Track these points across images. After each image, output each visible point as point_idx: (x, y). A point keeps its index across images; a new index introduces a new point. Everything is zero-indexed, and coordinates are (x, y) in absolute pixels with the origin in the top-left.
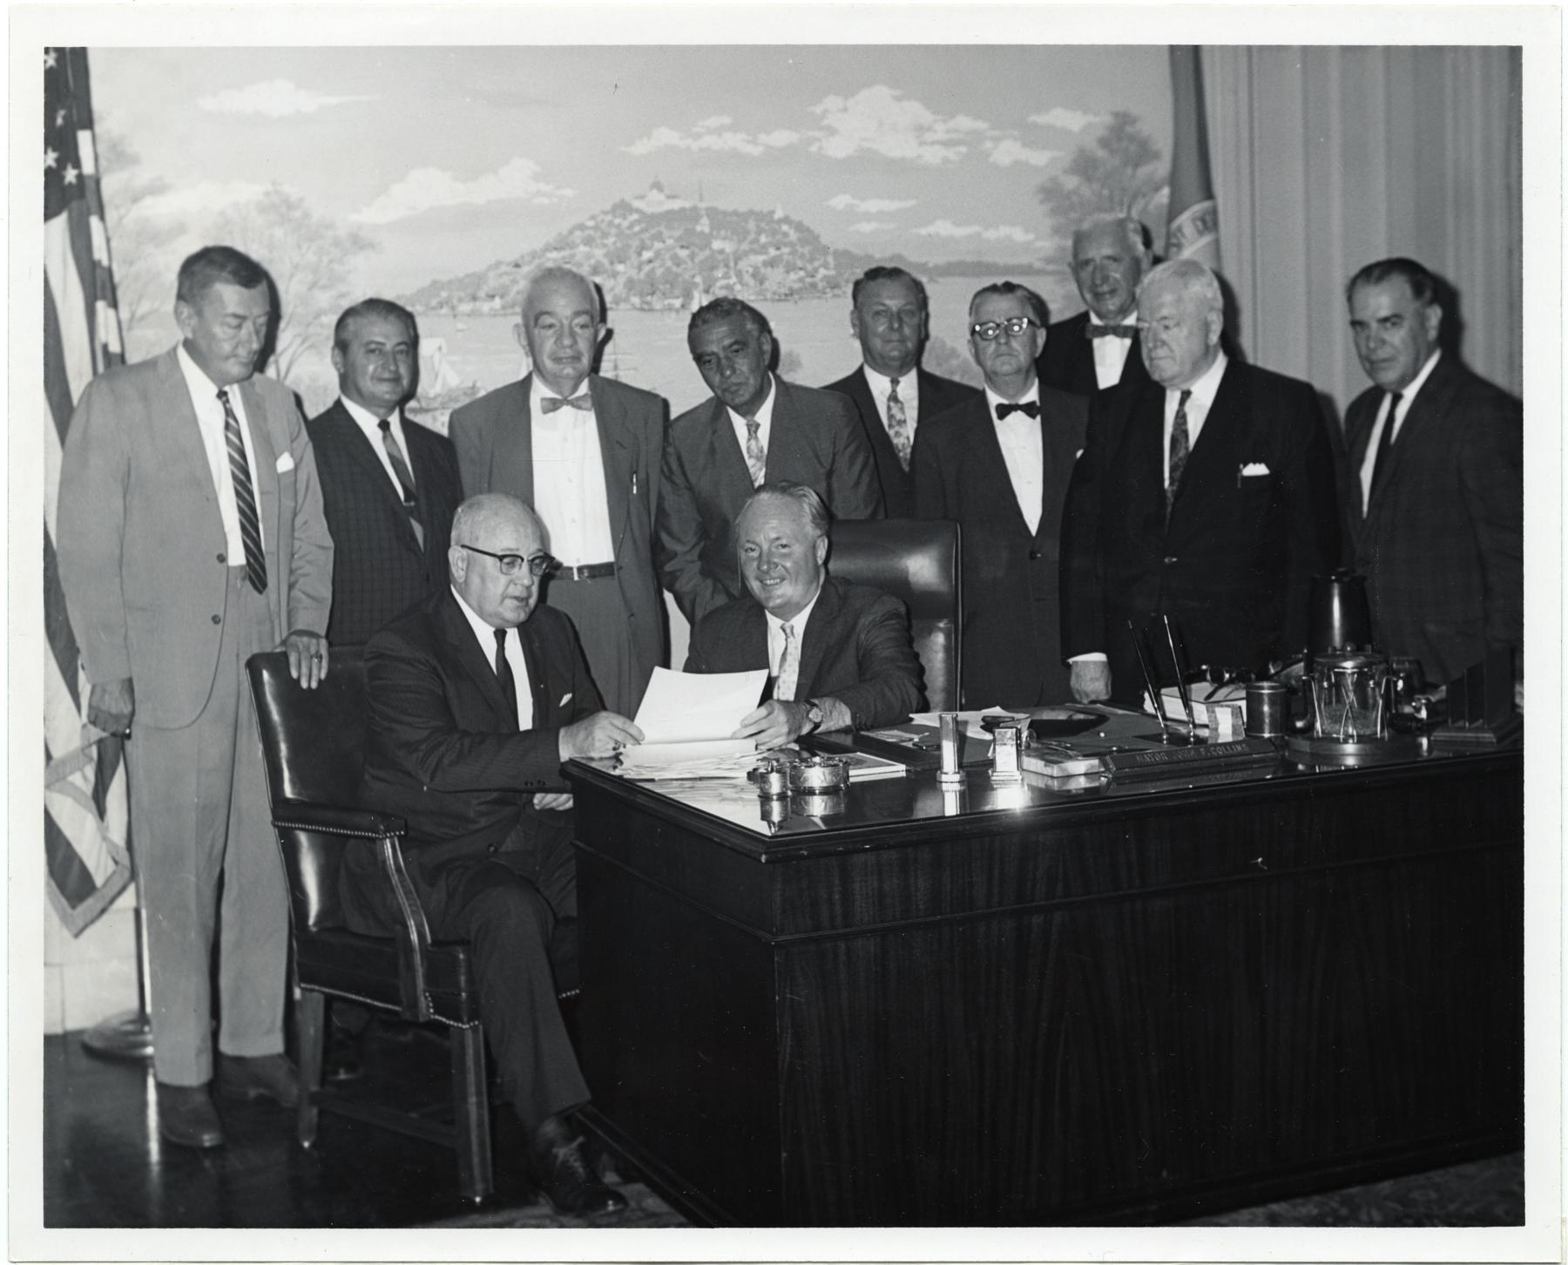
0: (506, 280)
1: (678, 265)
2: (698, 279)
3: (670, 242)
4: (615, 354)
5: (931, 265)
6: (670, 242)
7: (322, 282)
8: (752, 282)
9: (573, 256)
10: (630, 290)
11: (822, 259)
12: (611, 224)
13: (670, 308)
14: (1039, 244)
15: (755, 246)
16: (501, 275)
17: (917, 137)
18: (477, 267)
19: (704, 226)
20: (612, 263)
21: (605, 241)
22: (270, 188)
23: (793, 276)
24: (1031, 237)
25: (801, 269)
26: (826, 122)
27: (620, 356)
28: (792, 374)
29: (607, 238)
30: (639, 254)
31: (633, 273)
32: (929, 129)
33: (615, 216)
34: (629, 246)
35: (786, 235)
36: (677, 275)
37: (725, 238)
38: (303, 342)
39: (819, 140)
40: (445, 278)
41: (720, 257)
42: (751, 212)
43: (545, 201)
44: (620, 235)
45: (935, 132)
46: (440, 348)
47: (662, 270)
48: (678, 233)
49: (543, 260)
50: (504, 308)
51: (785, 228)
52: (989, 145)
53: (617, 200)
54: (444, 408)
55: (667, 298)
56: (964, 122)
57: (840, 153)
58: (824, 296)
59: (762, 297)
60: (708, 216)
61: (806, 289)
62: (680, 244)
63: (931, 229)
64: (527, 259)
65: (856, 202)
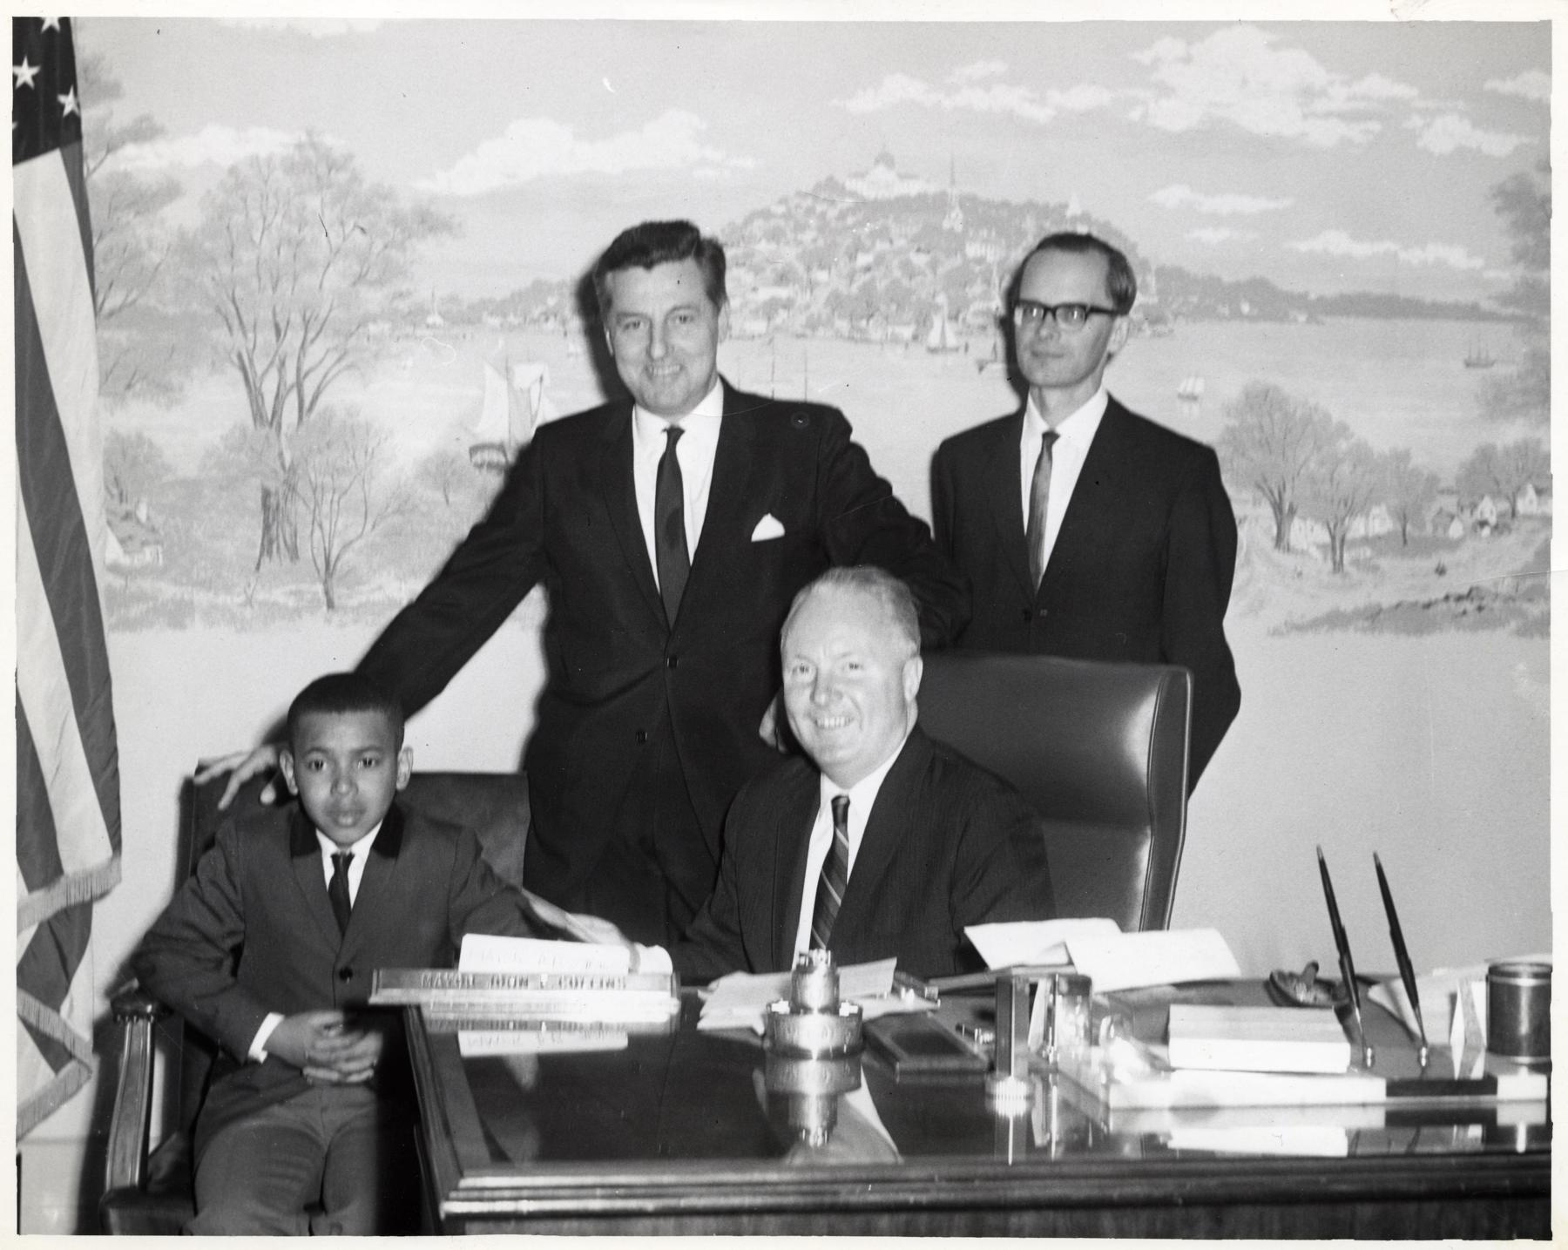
1: (911, 279)
2: (941, 299)
3: (901, 243)
5: (1313, 296)
10: (833, 310)
12: (810, 211)
13: (895, 340)
14: (1491, 274)
19: (954, 220)
20: (809, 269)
22: (304, 138)
24: (1478, 263)
30: (852, 257)
31: (842, 287)
32: (1323, 93)
37: (986, 241)
38: (339, 360)
41: (977, 269)
42: (1030, 206)
44: (823, 228)
46: (541, 379)
48: (913, 230)
52: (1417, 121)
56: (1378, 86)
62: (916, 247)
63: (1317, 244)
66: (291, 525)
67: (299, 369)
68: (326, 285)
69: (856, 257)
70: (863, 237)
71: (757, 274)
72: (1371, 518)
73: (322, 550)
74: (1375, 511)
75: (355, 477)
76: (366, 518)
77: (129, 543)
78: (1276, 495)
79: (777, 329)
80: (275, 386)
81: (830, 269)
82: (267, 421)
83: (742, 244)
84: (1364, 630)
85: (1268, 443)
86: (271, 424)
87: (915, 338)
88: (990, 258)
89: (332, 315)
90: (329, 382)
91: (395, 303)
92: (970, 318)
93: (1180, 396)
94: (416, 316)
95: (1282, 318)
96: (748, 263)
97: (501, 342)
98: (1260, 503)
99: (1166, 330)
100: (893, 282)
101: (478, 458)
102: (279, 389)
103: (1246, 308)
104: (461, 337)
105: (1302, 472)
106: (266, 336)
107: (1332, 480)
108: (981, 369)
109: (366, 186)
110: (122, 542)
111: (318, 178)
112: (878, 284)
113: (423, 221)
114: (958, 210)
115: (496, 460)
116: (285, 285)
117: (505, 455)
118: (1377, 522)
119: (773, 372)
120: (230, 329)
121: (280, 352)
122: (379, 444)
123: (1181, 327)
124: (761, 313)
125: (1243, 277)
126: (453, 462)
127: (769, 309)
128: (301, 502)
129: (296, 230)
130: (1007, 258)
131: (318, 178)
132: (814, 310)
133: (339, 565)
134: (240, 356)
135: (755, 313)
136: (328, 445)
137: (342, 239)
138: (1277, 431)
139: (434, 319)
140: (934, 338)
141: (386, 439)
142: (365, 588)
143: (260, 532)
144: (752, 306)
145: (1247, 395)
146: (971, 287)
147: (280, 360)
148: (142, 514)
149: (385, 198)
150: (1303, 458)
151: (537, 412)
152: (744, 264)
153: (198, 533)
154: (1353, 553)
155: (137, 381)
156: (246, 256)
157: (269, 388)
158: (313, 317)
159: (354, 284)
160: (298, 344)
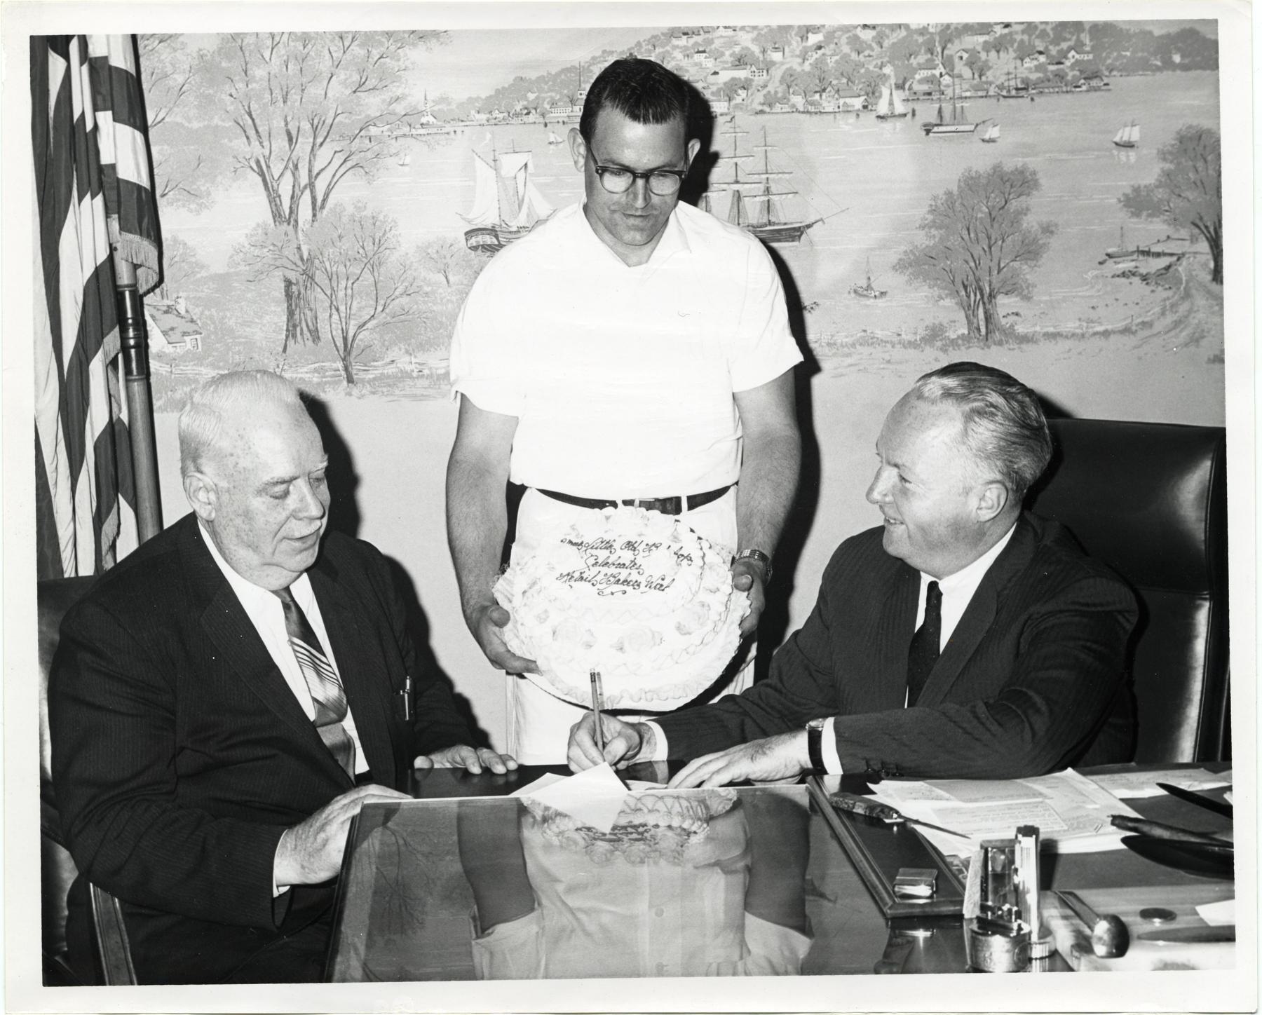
1: (859, 53)
4: (767, 173)
7: (369, 85)
8: (967, 73)
9: (711, 42)
10: (789, 87)
11: (1074, 38)
20: (764, 52)
23: (1029, 63)
25: (1041, 53)
27: (771, 176)
28: (1023, 198)
30: (804, 38)
31: (795, 64)
38: (345, 161)
40: (533, 75)
41: (921, 40)
46: (526, 165)
58: (1078, 89)
59: (980, 93)
61: (1049, 81)
66: (311, 310)
67: (310, 171)
68: (328, 95)
69: (807, 38)
71: (716, 59)
73: (340, 332)
76: (377, 302)
77: (170, 333)
78: (1212, 230)
79: (737, 106)
80: (291, 188)
82: (285, 218)
85: (1202, 182)
86: (289, 224)
87: (865, 107)
89: (336, 121)
91: (391, 108)
92: (916, 87)
93: (1117, 144)
94: (411, 117)
96: (707, 50)
98: (1197, 239)
99: (1102, 84)
100: (841, 58)
101: (473, 242)
102: (294, 192)
103: (1177, 58)
104: (452, 133)
106: (280, 143)
108: (928, 132)
110: (165, 333)
112: (829, 61)
115: (489, 243)
116: (294, 96)
117: (496, 236)
119: (736, 150)
120: (248, 138)
121: (294, 158)
122: (384, 234)
123: (1116, 80)
124: (722, 93)
126: (451, 246)
128: (319, 290)
129: (302, 48)
132: (771, 88)
134: (258, 162)
136: (340, 237)
137: (342, 51)
140: (883, 108)
141: (391, 230)
143: (285, 318)
144: (714, 88)
146: (915, 58)
147: (293, 162)
148: (181, 308)
152: (704, 52)
153: (232, 323)
155: (169, 191)
156: (259, 72)
157: (285, 190)
158: (321, 122)
159: (355, 92)
160: (309, 148)
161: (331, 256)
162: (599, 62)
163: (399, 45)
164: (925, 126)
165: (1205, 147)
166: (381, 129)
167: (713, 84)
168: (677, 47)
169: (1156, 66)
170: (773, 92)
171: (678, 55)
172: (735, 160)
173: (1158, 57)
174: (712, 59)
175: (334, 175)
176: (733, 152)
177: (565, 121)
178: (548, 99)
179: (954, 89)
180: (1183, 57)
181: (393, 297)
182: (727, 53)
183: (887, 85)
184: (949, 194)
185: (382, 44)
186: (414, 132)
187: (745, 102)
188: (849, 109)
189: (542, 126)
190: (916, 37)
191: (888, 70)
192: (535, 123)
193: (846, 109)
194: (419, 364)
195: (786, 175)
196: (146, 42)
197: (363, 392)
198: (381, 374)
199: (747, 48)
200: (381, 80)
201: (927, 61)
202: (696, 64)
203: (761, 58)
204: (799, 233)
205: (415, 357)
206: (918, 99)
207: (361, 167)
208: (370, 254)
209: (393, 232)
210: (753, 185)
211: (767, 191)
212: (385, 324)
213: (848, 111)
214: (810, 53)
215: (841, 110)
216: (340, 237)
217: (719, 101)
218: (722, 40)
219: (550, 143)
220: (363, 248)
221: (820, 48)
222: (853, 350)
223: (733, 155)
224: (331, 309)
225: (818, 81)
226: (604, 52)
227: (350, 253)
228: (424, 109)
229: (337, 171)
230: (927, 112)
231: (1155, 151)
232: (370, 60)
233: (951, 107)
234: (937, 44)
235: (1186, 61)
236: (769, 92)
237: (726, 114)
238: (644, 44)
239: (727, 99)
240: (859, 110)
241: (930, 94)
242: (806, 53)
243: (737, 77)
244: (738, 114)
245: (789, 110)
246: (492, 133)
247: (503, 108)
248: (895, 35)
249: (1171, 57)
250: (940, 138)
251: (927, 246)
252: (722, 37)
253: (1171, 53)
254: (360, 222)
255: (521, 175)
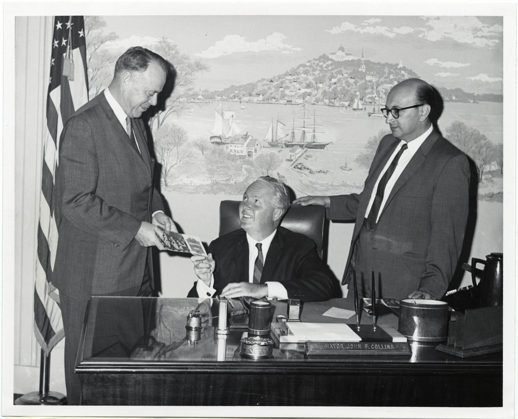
0: (266, 87)
1: (348, 87)
2: (358, 93)
4: (314, 125)
5: (475, 95)
6: (345, 75)
9: (299, 78)
10: (324, 96)
13: (343, 106)
15: (388, 80)
16: (263, 85)
17: (473, 34)
18: (253, 80)
20: (316, 83)
21: (314, 73)
22: (162, 40)
26: (428, 24)
27: (316, 126)
29: (315, 72)
30: (330, 80)
31: (327, 88)
32: (481, 30)
33: (320, 62)
34: (326, 76)
35: (403, 75)
36: (348, 91)
37: (373, 76)
38: (170, 109)
39: (424, 32)
40: (237, 86)
41: (369, 84)
42: (387, 64)
43: (287, 52)
45: (483, 32)
46: (233, 116)
47: (341, 88)
49: (284, 79)
50: (263, 100)
51: (403, 72)
53: (322, 55)
54: (232, 144)
55: (341, 101)
57: (434, 39)
60: (365, 65)
62: (350, 77)
63: (477, 78)
64: (277, 78)
65: (441, 62)
69: (331, 80)
70: (334, 74)
71: (300, 85)
72: (491, 165)
74: (493, 163)
75: (175, 146)
79: (306, 102)
81: (323, 84)
83: (296, 75)
84: (488, 200)
85: (459, 140)
87: (349, 105)
88: (373, 81)
90: (167, 117)
92: (367, 100)
94: (195, 96)
95: (466, 101)
96: (297, 81)
97: (221, 105)
101: (213, 140)
103: (454, 98)
104: (208, 103)
105: (470, 150)
107: (479, 153)
108: (370, 115)
109: (180, 55)
111: (166, 52)
113: (197, 67)
114: (364, 65)
115: (218, 141)
118: (493, 166)
119: (304, 116)
122: (182, 136)
124: (301, 96)
125: (453, 88)
126: (205, 141)
127: (304, 96)
130: (379, 80)
131: (166, 52)
132: (318, 96)
133: (170, 172)
135: (299, 97)
138: (463, 137)
139: (200, 97)
140: (355, 106)
142: (177, 180)
144: (299, 95)
145: (454, 125)
149: (186, 59)
150: (470, 146)
151: (231, 127)
152: (296, 82)
154: (486, 176)
161: (163, 142)
162: (260, 82)
163: (192, 71)
164: (369, 113)
165: (461, 129)
166: (184, 99)
167: (298, 93)
168: (286, 79)
169: (447, 100)
170: (318, 98)
171: (287, 82)
172: (304, 120)
173: (448, 97)
174: (299, 84)
175: (166, 114)
176: (303, 116)
177: (248, 101)
178: (242, 94)
179: (379, 103)
180: (456, 97)
181: (184, 157)
182: (304, 83)
183: (357, 98)
184: (375, 137)
185: (186, 70)
186: (195, 101)
187: (309, 100)
188: (344, 105)
189: (239, 102)
190: (368, 83)
191: (358, 93)
192: (237, 101)
193: (343, 105)
194: (192, 181)
195: (321, 127)
196: (105, 63)
197: (171, 190)
198: (178, 184)
199: (311, 82)
200: (185, 82)
201: (372, 91)
202: (293, 86)
203: (315, 86)
204: (323, 146)
205: (190, 179)
206: (367, 104)
207: (176, 112)
208: (177, 142)
209: (185, 135)
210: (310, 129)
211: (314, 131)
212: (180, 167)
213: (343, 106)
214: (332, 85)
215: (341, 105)
216: (167, 135)
217: (300, 99)
218: (303, 78)
219: (242, 109)
220: (174, 140)
221: (335, 84)
222: (339, 188)
223: (303, 118)
224: (161, 159)
225: (334, 95)
226: (262, 79)
227: (170, 141)
228: (199, 93)
229: (167, 112)
230: (370, 109)
231: (445, 129)
232: (182, 75)
233: (378, 108)
234: (375, 86)
235: (457, 99)
236: (317, 97)
237: (302, 104)
238: (276, 77)
239: (303, 98)
240: (347, 106)
241: (371, 103)
242: (331, 85)
243: (307, 91)
244: (307, 104)
245: (324, 104)
246: (222, 104)
247: (226, 95)
248: (361, 81)
249: (452, 98)
250: (374, 118)
251: (367, 155)
252: (303, 77)
253: (452, 96)
254: (174, 131)
255: (231, 119)
